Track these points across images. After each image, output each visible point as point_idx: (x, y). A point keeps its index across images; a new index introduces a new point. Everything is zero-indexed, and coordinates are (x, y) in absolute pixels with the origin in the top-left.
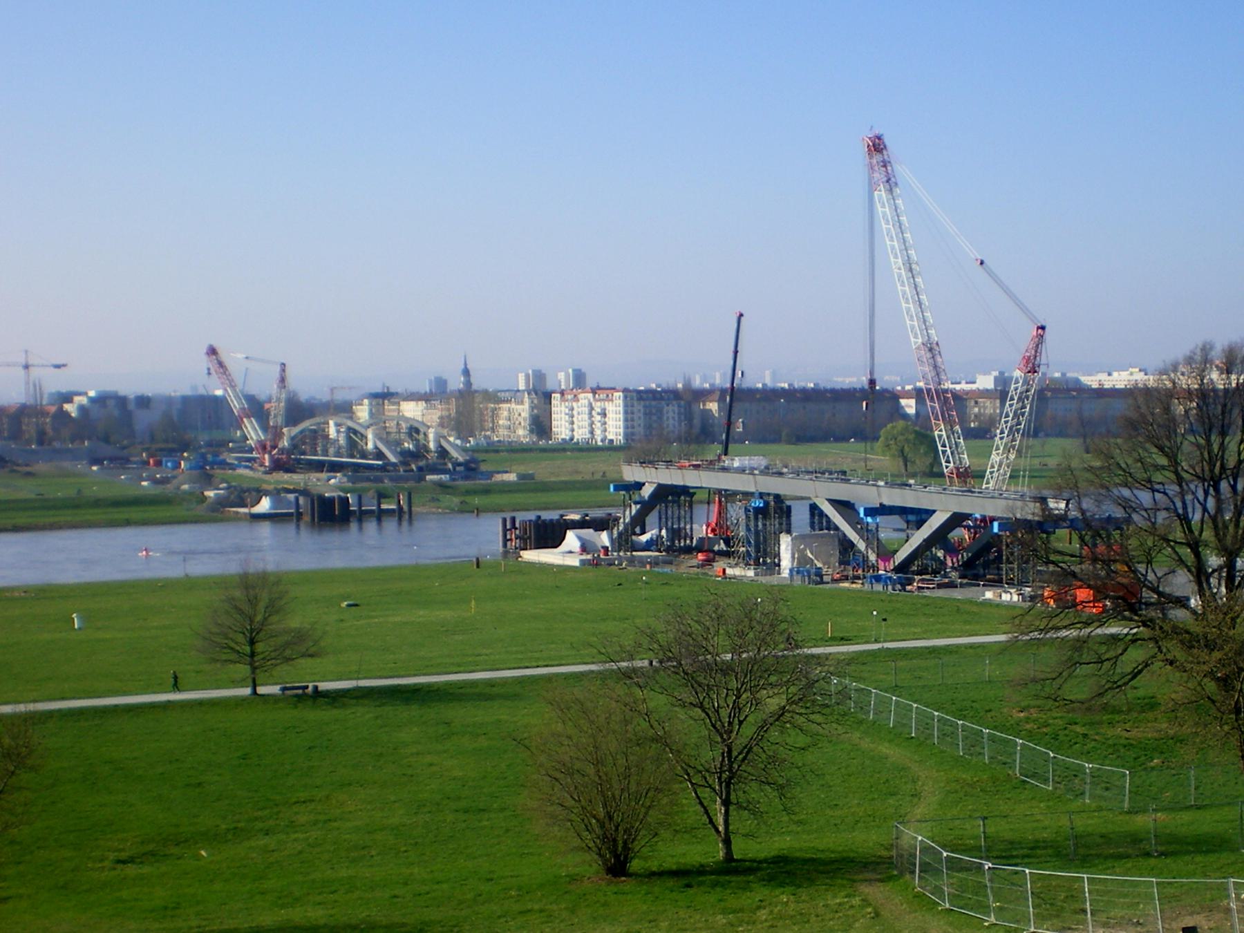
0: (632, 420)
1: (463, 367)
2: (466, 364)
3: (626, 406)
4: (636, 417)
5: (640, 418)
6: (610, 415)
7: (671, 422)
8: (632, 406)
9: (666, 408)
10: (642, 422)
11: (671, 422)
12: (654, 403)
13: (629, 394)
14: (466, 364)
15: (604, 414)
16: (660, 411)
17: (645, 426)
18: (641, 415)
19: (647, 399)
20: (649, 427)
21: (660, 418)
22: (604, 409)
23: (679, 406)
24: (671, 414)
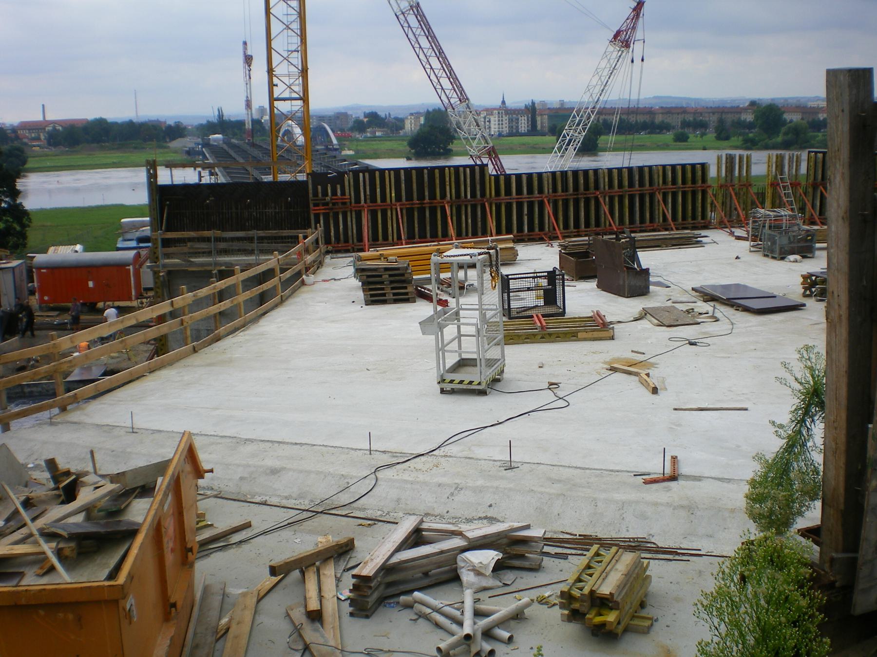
0: (502, 124)
1: (502, 99)
2: (503, 98)
3: (499, 117)
4: (504, 123)
5: (506, 123)
6: (492, 122)
7: (523, 125)
8: (502, 117)
9: (520, 118)
10: (507, 125)
11: (523, 125)
12: (514, 116)
13: (500, 111)
14: (503, 98)
15: (489, 121)
16: (518, 119)
17: (509, 127)
18: (507, 121)
19: (511, 114)
20: (511, 127)
21: (518, 123)
22: (490, 119)
23: (528, 117)
24: (523, 121)
